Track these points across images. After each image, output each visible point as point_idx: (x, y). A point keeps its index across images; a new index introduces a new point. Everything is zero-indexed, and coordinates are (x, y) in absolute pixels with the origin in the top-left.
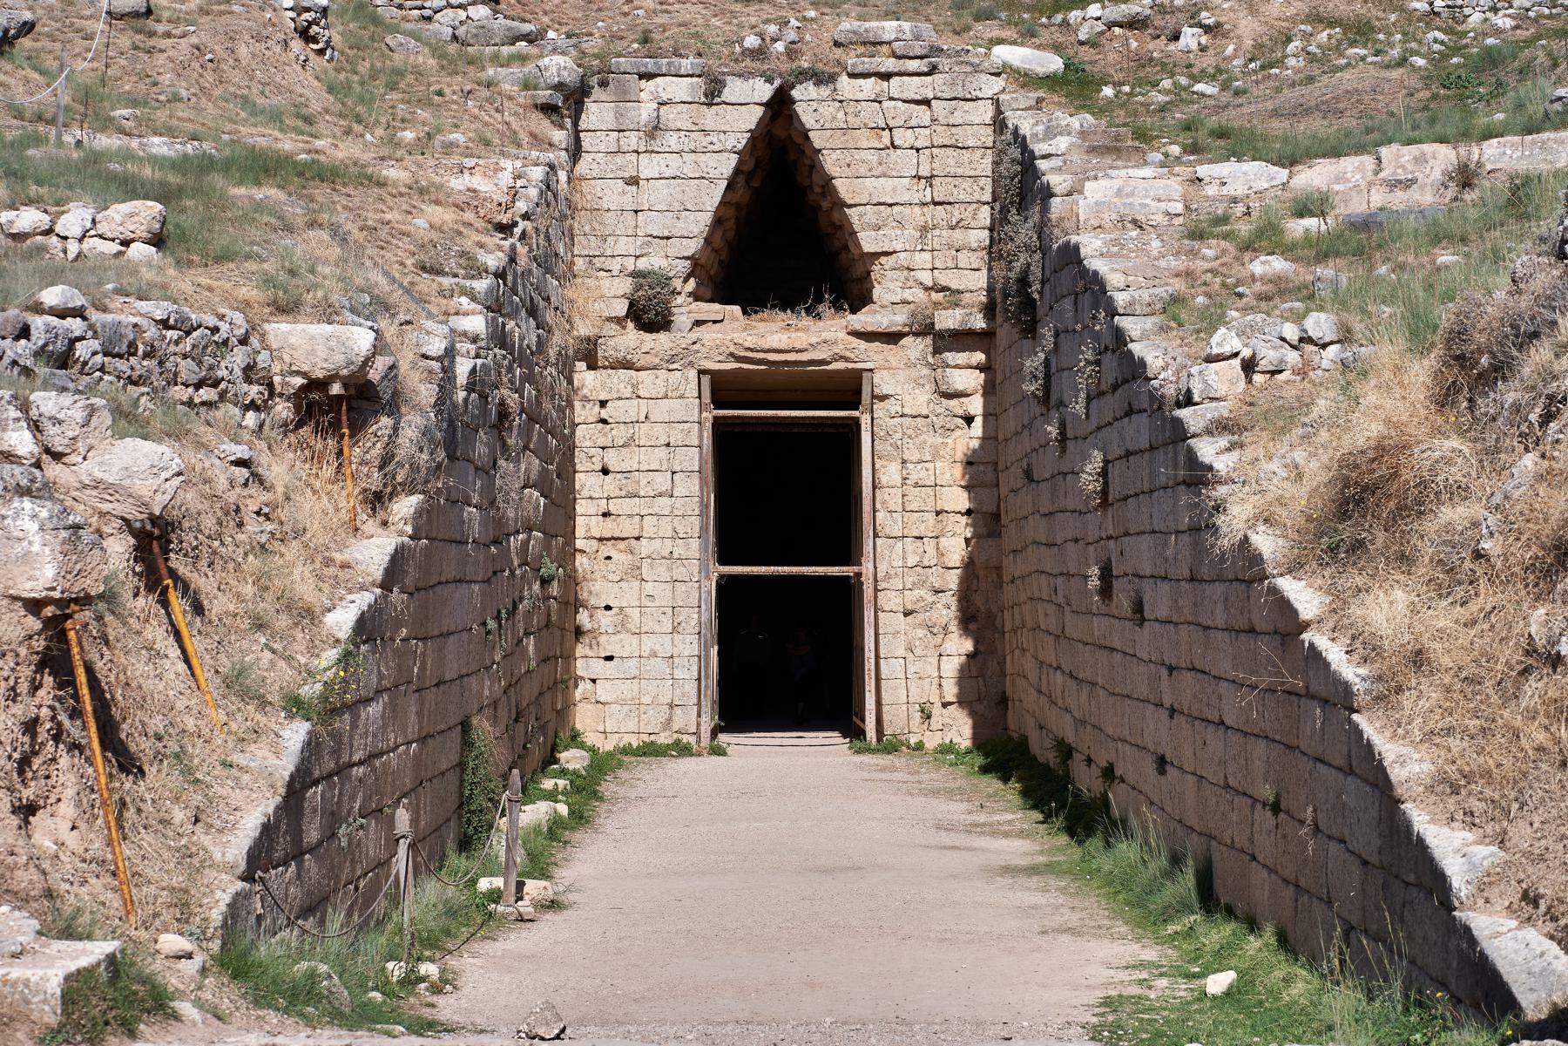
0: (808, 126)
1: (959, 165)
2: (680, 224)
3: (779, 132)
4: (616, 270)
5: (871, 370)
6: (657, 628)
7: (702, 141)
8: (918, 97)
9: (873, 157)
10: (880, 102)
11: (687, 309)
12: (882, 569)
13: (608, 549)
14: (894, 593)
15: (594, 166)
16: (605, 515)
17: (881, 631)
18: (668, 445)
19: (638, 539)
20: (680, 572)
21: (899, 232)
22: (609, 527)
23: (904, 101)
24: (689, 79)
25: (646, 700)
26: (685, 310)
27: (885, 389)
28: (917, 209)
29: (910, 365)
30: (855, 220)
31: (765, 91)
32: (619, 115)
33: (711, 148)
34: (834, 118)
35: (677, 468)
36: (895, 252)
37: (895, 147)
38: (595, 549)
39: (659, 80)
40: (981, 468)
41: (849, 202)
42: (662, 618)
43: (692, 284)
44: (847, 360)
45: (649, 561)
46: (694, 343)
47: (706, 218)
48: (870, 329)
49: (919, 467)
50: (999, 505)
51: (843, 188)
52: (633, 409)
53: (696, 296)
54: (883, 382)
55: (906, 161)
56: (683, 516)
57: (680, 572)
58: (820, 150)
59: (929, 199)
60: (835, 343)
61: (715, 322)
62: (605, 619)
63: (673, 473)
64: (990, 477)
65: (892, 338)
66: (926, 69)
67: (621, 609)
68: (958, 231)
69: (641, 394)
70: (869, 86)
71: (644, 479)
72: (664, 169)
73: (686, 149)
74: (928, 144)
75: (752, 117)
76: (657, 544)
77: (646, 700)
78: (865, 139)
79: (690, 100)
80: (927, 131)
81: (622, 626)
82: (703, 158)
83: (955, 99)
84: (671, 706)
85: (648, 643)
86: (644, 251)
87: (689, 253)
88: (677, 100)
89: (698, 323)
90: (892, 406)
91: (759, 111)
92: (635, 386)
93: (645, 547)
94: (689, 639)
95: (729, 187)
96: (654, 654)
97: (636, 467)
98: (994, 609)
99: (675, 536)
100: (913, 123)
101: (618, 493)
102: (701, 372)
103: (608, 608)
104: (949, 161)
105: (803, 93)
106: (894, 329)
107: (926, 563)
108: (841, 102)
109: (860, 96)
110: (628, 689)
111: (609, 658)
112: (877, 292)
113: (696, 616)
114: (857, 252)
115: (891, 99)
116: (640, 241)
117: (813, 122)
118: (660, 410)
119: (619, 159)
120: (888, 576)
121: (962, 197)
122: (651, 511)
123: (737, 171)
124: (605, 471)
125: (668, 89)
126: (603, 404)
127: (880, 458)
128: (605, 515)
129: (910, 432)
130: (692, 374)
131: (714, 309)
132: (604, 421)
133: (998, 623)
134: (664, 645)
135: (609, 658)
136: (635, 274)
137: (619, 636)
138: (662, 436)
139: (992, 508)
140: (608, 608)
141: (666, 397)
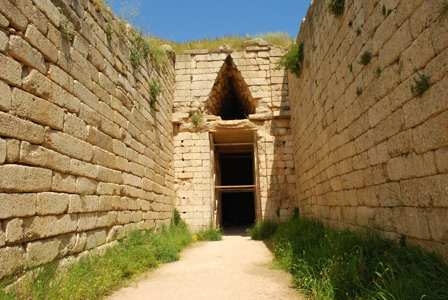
0: (236, 65)
2: (203, 93)
3: (230, 74)
5: (256, 130)
6: (198, 203)
7: (208, 70)
8: (266, 57)
10: (255, 59)
11: (206, 116)
13: (185, 182)
14: (265, 192)
15: (179, 78)
16: (183, 172)
17: (262, 203)
18: (200, 152)
19: (192, 178)
20: (204, 187)
21: (262, 92)
23: (262, 58)
24: (204, 55)
27: (261, 135)
28: (267, 87)
30: (250, 90)
31: (224, 56)
33: (210, 72)
34: (243, 63)
35: (203, 159)
36: (261, 98)
37: (259, 70)
38: (180, 182)
39: (196, 56)
40: (289, 155)
41: (249, 85)
42: (199, 200)
45: (196, 184)
46: (207, 125)
47: (210, 91)
48: (255, 118)
49: (271, 156)
50: (294, 166)
51: (247, 81)
52: (191, 142)
55: (263, 74)
56: (205, 172)
57: (204, 187)
58: (240, 71)
59: (270, 83)
60: (246, 123)
61: (213, 120)
62: (183, 201)
63: (202, 160)
64: (291, 157)
65: (260, 121)
66: (267, 49)
67: (188, 198)
68: (278, 91)
69: (193, 139)
70: (253, 55)
71: (193, 162)
72: (198, 78)
73: (204, 73)
74: (269, 69)
75: (221, 63)
76: (198, 180)
79: (204, 60)
80: (269, 66)
81: (188, 203)
82: (208, 75)
83: (275, 57)
85: (196, 208)
86: (193, 100)
87: (205, 100)
88: (201, 60)
89: (208, 120)
90: (263, 140)
91: (223, 62)
92: (191, 136)
93: (194, 181)
94: (207, 206)
97: (191, 158)
98: (294, 195)
100: (265, 63)
101: (186, 166)
102: (210, 133)
103: (184, 198)
106: (262, 118)
107: (274, 183)
108: (245, 59)
109: (250, 57)
111: (185, 212)
112: (257, 109)
113: (209, 200)
115: (258, 57)
116: (192, 98)
117: (237, 64)
118: (198, 143)
119: (186, 76)
121: (279, 82)
122: (196, 171)
124: (183, 160)
125: (199, 58)
126: (182, 141)
127: (260, 154)
128: (183, 172)
129: (268, 146)
130: (207, 133)
131: (212, 117)
132: (183, 146)
133: (296, 199)
134: (200, 208)
135: (185, 212)
137: (187, 206)
139: (292, 166)
140: (184, 198)
141: (200, 139)
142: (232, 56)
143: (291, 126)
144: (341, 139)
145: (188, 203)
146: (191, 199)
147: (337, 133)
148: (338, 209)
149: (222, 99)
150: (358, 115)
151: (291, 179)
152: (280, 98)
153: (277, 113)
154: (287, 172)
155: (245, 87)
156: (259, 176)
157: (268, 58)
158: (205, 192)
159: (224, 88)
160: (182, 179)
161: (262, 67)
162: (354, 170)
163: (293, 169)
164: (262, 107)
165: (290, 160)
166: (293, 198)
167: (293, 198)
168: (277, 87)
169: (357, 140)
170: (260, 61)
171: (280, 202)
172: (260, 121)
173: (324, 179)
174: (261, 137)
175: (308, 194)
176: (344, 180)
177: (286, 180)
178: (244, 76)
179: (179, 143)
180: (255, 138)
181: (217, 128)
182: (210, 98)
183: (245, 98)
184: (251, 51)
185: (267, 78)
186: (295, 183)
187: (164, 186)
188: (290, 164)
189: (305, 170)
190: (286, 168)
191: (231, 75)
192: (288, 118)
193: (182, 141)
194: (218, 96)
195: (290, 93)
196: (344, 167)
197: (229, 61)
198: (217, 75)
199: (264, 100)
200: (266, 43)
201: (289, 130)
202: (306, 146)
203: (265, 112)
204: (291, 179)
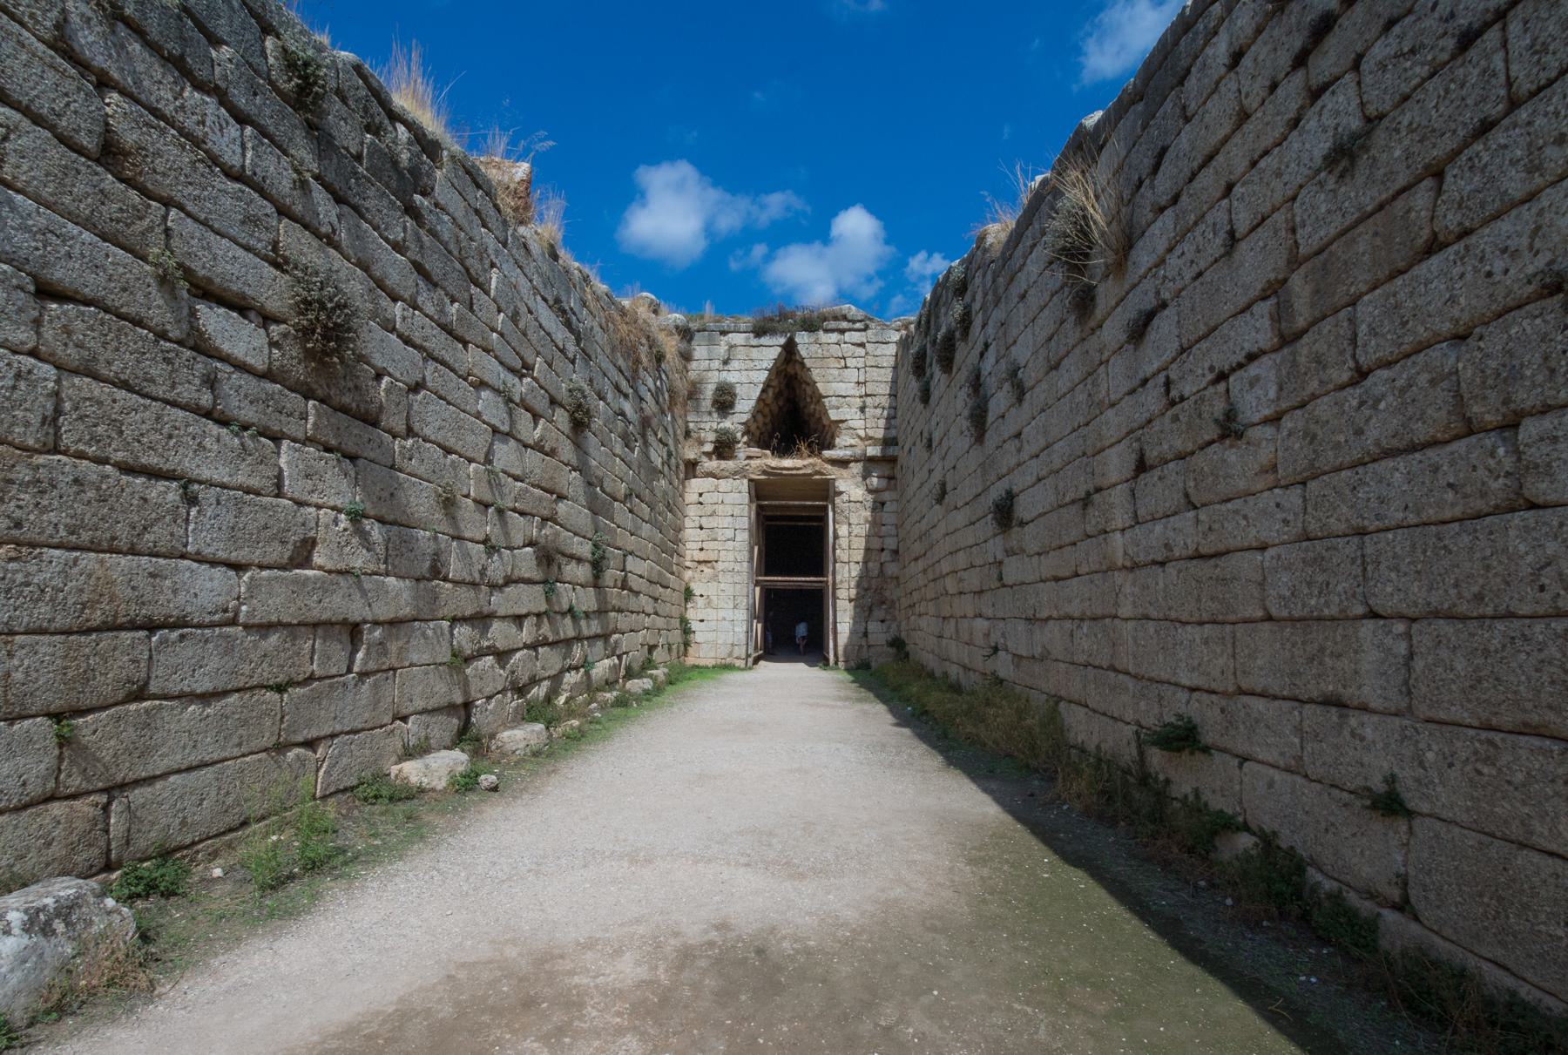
1: (879, 375)
3: (791, 371)
4: (707, 428)
7: (752, 365)
9: (836, 372)
12: (838, 578)
13: (702, 567)
16: (701, 549)
20: (737, 578)
22: (702, 556)
25: (720, 642)
26: (742, 451)
27: (842, 489)
29: (854, 477)
31: (782, 341)
32: (710, 352)
37: (846, 367)
43: (745, 439)
44: (823, 474)
47: (753, 403)
52: (715, 497)
53: (748, 444)
54: (841, 485)
64: (894, 532)
65: (843, 463)
70: (834, 337)
75: (774, 353)
76: (726, 564)
77: (720, 642)
78: (833, 363)
81: (709, 604)
84: (733, 645)
85: (722, 614)
89: (749, 458)
90: (845, 497)
91: (779, 349)
92: (717, 486)
93: (720, 566)
95: (763, 391)
96: (724, 619)
99: (736, 561)
102: (751, 480)
104: (874, 374)
105: (802, 338)
110: (711, 636)
111: (702, 621)
112: (837, 441)
114: (825, 422)
118: (729, 498)
120: (842, 582)
123: (769, 380)
124: (701, 528)
126: (701, 495)
128: (701, 549)
130: (745, 481)
131: (755, 451)
134: (729, 614)
135: (702, 621)
136: (716, 431)
138: (729, 510)
139: (894, 547)
142: (797, 340)
143: (899, 476)
144: (960, 518)
145: (709, 604)
146: (714, 598)
147: (956, 508)
148: (953, 622)
149: (772, 415)
150: (980, 490)
151: (892, 569)
152: (882, 423)
153: (873, 451)
154: (885, 556)
155: (819, 398)
156: (835, 561)
157: (862, 345)
158: (738, 586)
159: (777, 396)
160: (699, 562)
161: (850, 362)
162: (973, 566)
163: (896, 552)
164: (847, 438)
165: (890, 536)
166: (893, 602)
167: (893, 602)
168: (877, 400)
169: (977, 525)
170: (848, 349)
171: (870, 610)
172: (843, 463)
173: (938, 575)
174: (841, 493)
175: (916, 596)
176: (961, 580)
177: (881, 571)
178: (817, 379)
179: (695, 498)
180: (831, 494)
181: (764, 472)
182: (754, 417)
183: (817, 415)
184: (832, 331)
185: (858, 383)
186: (897, 578)
187: (673, 573)
188: (891, 543)
189: (913, 556)
190: (883, 550)
191: (792, 372)
192: (892, 460)
193: (701, 495)
194: (767, 410)
195: (899, 414)
196: (961, 560)
197: (790, 349)
198: (766, 374)
199: (851, 424)
200: (860, 314)
201: (893, 482)
202: (916, 517)
203: (851, 446)
204: (892, 569)
